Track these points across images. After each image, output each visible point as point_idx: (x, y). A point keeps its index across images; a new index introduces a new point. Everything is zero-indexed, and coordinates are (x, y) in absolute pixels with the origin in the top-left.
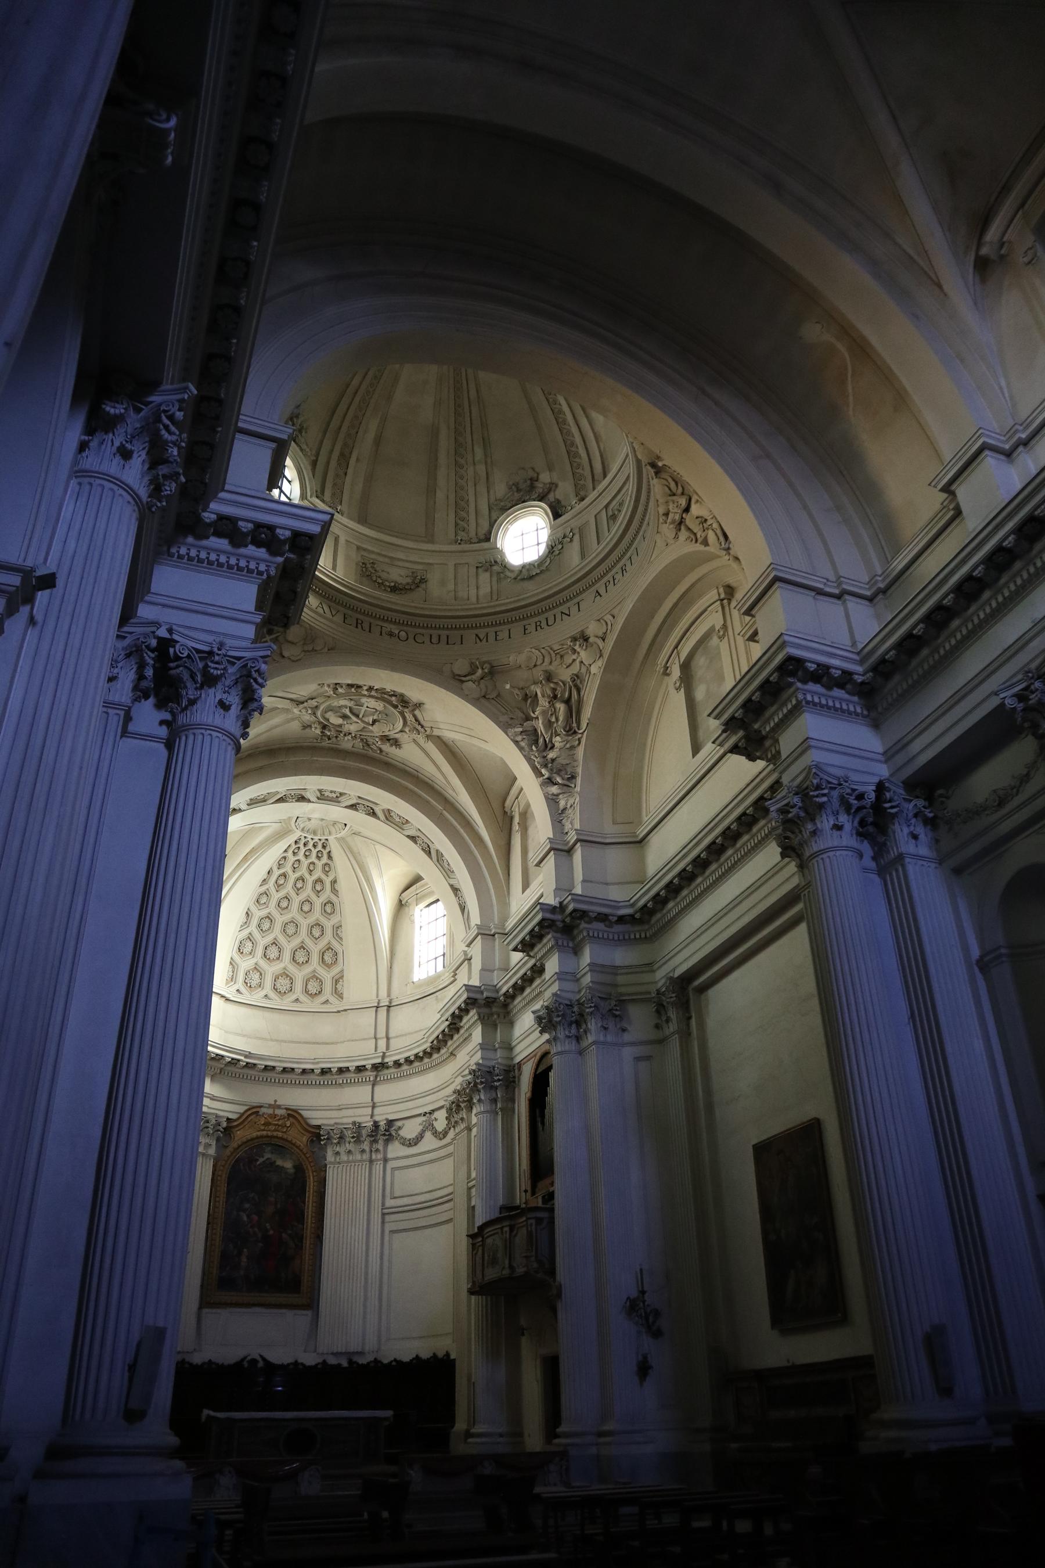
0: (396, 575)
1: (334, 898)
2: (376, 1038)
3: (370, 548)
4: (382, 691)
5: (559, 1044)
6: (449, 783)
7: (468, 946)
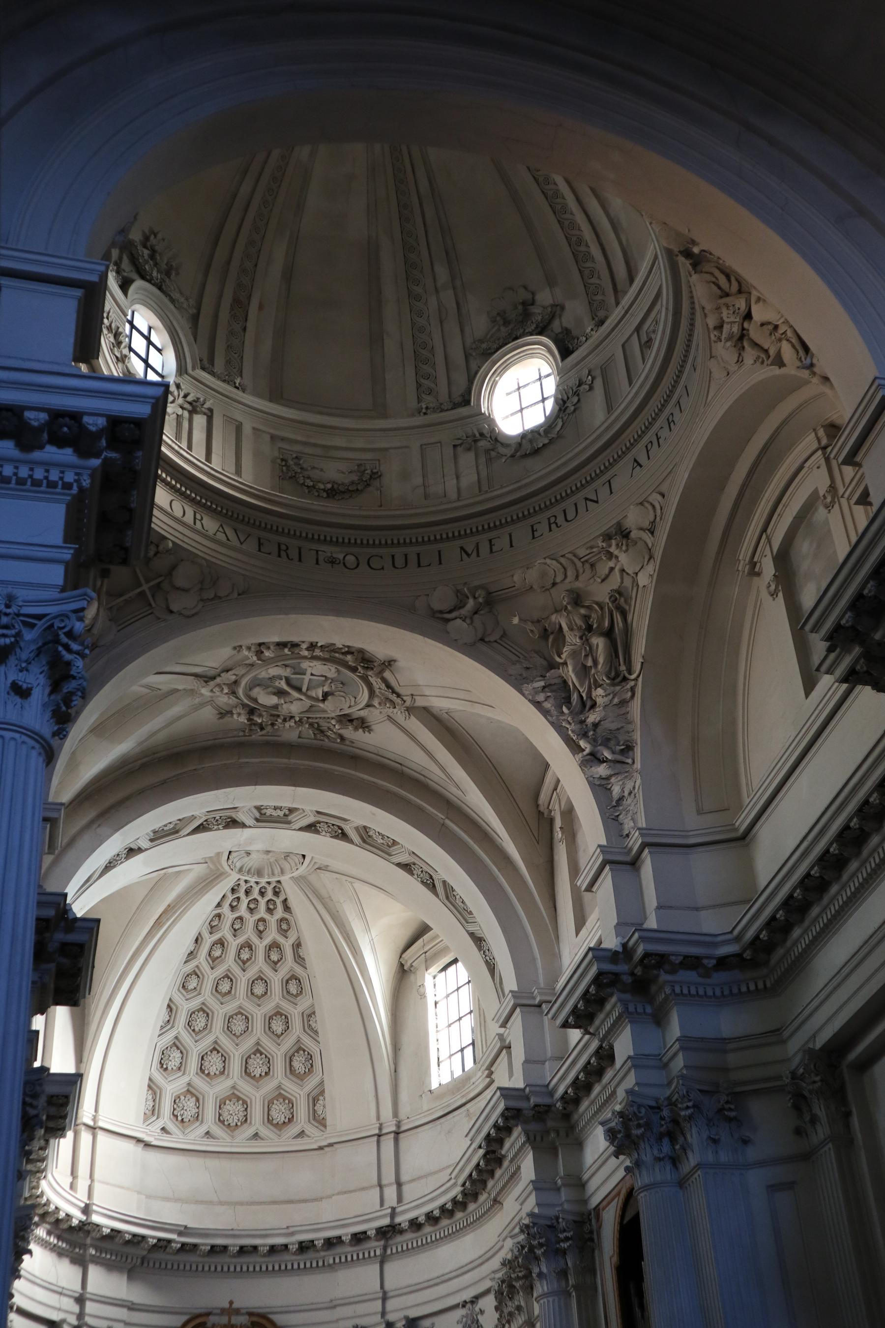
0: (334, 471)
1: (299, 970)
2: (381, 1186)
3: (292, 436)
4: (330, 648)
5: (644, 1173)
6: (450, 777)
7: (504, 1025)
